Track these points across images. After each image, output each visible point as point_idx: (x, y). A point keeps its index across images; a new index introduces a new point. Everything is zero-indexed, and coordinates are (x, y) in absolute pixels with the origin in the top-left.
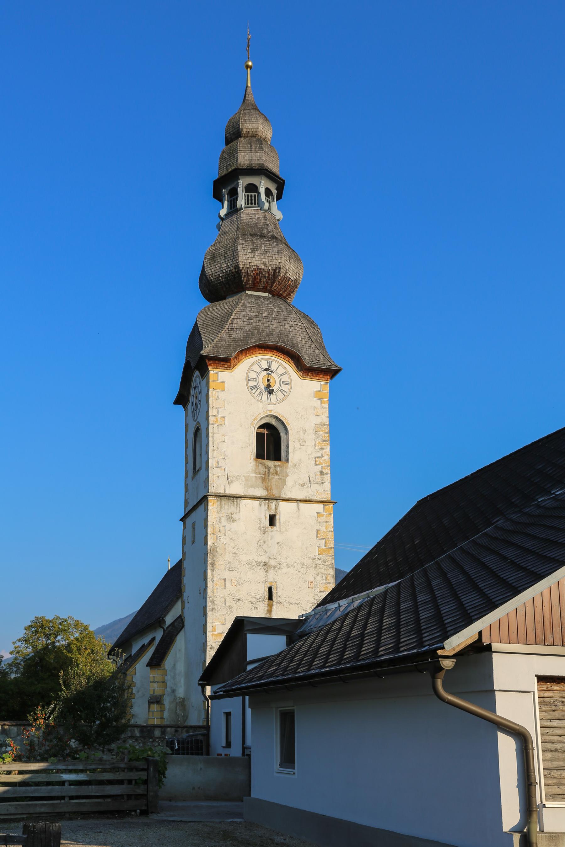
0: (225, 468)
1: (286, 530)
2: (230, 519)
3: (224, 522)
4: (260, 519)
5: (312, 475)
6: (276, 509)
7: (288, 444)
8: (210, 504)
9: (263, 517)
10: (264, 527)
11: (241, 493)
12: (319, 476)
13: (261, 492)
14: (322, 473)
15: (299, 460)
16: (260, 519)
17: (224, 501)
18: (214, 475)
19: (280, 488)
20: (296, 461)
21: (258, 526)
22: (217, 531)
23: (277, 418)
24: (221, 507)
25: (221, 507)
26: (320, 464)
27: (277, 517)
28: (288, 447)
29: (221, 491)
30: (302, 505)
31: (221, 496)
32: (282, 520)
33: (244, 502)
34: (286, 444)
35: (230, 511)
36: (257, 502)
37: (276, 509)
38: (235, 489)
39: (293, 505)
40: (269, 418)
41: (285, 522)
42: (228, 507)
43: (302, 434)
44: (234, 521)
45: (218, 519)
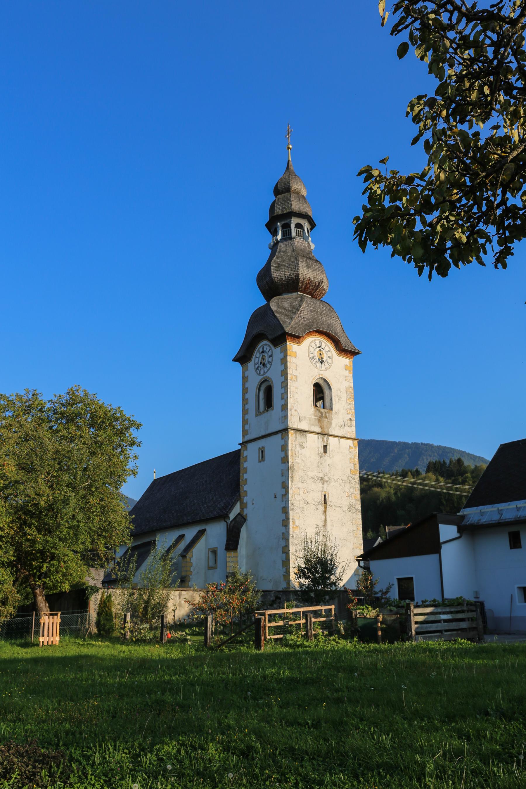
0: (297, 411)
1: (333, 456)
2: (302, 446)
3: (298, 448)
4: (318, 448)
5: (346, 421)
6: (327, 441)
7: (332, 398)
8: (290, 435)
9: (320, 447)
10: (321, 453)
11: (307, 429)
12: (349, 421)
13: (318, 429)
14: (350, 419)
15: (338, 410)
16: (318, 448)
17: (298, 433)
18: (292, 415)
19: (329, 428)
20: (336, 410)
21: (317, 453)
22: (294, 454)
23: (325, 380)
24: (296, 438)
25: (296, 438)
26: (350, 414)
27: (328, 447)
28: (331, 400)
29: (295, 427)
30: (342, 440)
31: (296, 430)
32: (330, 450)
33: (309, 435)
34: (330, 398)
35: (301, 441)
36: (316, 436)
37: (327, 441)
38: (304, 426)
39: (336, 439)
40: (320, 380)
41: (332, 451)
42: (300, 438)
43: (339, 392)
44: (303, 448)
45: (294, 445)
